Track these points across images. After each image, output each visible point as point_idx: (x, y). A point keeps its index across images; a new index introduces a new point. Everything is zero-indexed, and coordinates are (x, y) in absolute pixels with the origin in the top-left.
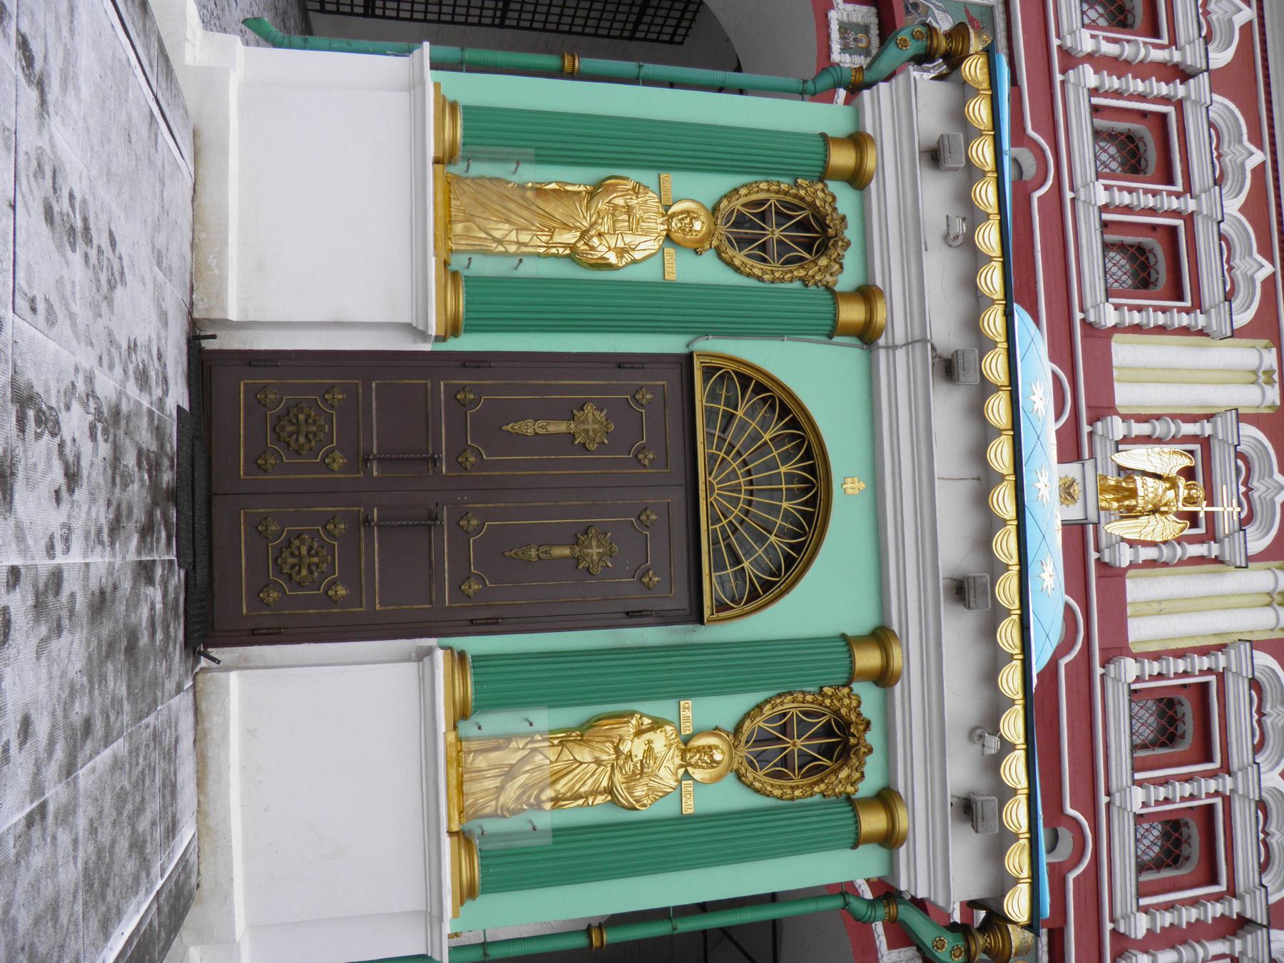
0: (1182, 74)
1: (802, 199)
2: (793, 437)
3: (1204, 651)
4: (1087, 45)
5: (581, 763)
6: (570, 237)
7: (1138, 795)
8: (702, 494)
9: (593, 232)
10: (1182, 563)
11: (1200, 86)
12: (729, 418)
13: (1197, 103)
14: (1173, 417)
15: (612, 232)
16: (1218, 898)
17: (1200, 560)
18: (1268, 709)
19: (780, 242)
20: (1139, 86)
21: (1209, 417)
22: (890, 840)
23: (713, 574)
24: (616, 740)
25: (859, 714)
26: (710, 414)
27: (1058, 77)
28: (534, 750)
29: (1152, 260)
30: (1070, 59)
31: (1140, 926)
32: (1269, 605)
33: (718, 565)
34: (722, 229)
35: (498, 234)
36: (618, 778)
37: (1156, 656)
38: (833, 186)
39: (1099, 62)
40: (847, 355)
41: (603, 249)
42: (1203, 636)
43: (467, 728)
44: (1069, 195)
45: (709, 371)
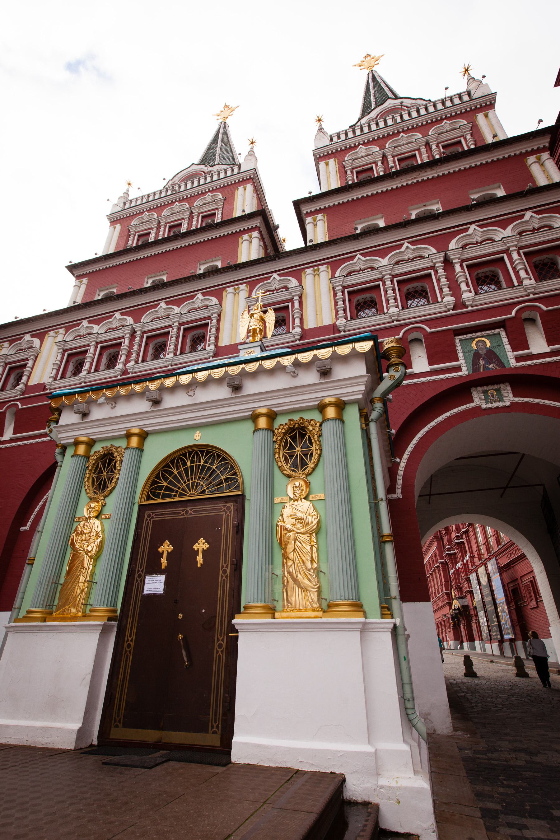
1: (94, 464)
2: (178, 461)
3: (335, 295)
5: (295, 549)
7: (393, 310)
9: (86, 549)
11: (138, 327)
12: (167, 489)
13: (143, 327)
15: (88, 541)
16: (436, 272)
17: (301, 303)
19: (107, 473)
20: (136, 347)
22: (341, 406)
23: (225, 491)
24: (286, 532)
25: (286, 424)
26: (165, 496)
27: (131, 375)
28: (289, 572)
29: (197, 336)
31: (450, 299)
32: (319, 275)
35: (79, 591)
36: (302, 530)
37: (337, 312)
38: (92, 453)
40: (150, 443)
42: (330, 297)
45: (148, 498)
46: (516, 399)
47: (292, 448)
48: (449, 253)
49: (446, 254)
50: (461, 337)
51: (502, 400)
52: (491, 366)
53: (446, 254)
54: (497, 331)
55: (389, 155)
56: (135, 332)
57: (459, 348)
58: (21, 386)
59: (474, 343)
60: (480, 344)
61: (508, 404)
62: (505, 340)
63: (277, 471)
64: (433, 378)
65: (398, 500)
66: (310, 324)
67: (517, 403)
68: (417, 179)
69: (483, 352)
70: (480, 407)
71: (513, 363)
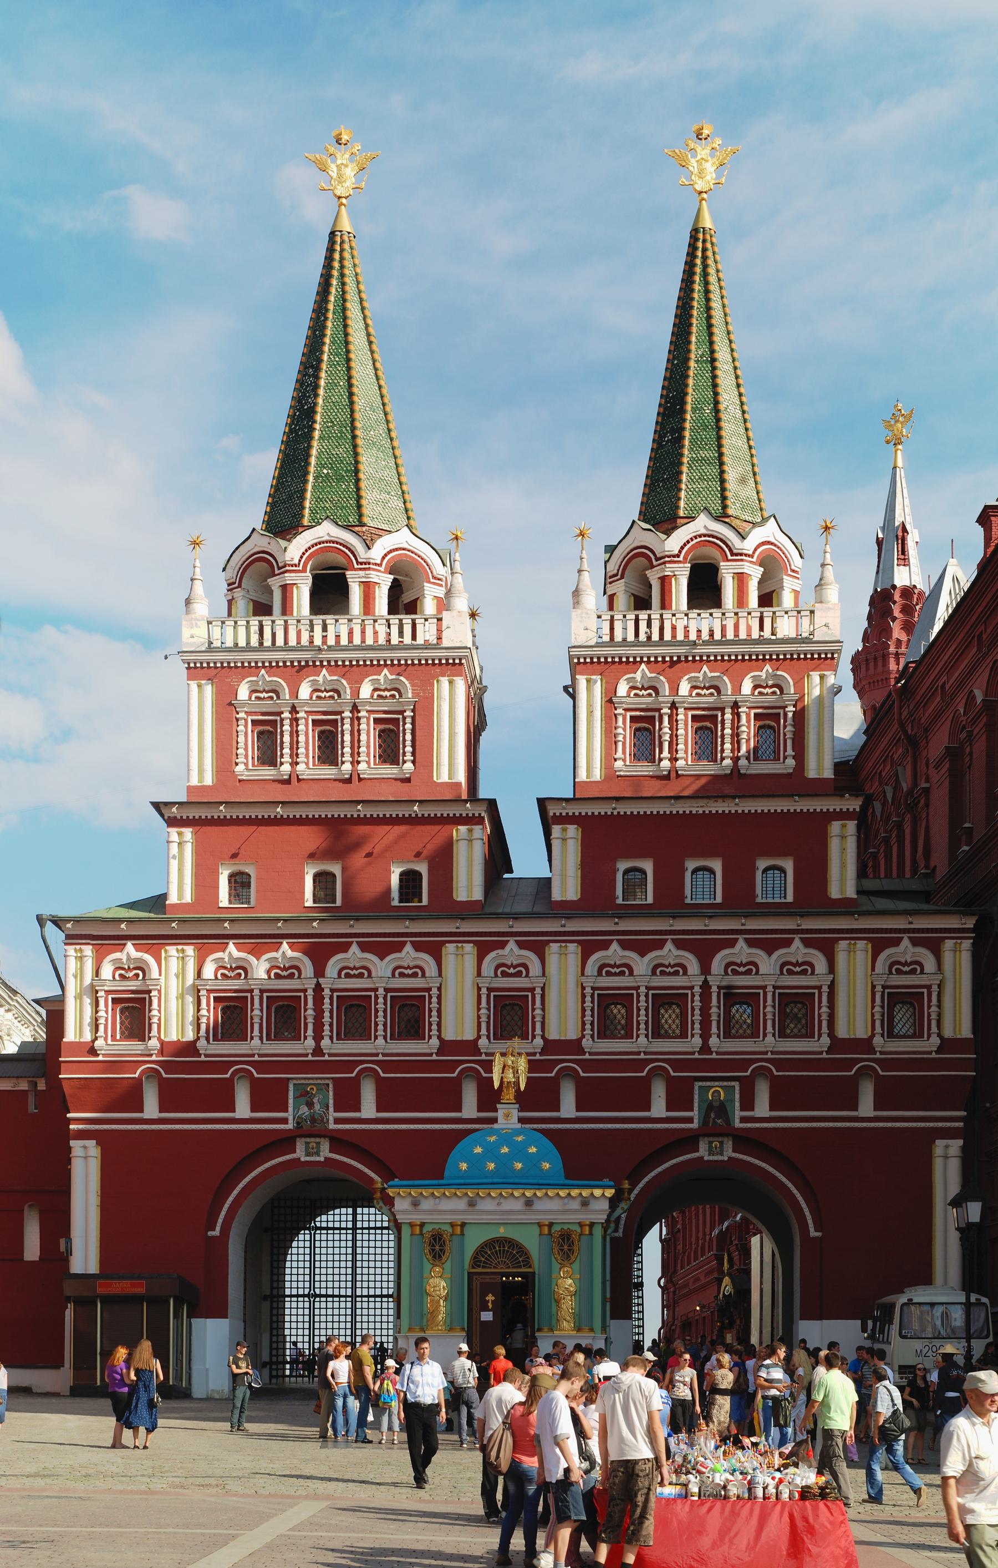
0: (318, 989)
3: (583, 996)
4: (310, 1043)
6: (442, 1301)
8: (503, 1270)
10: (543, 1009)
14: (479, 1009)
18: (612, 963)
21: (479, 989)
26: (484, 1267)
30: (318, 1051)
33: (520, 1267)
34: (437, 1262)
37: (584, 1024)
39: (318, 1037)
41: (444, 1293)
43: (554, 1329)
44: (380, 1058)
45: (473, 1268)
46: (734, 1155)
47: (562, 1246)
48: (709, 978)
49: (706, 979)
50: (701, 1084)
51: (722, 1154)
52: (719, 1121)
53: (706, 979)
54: (733, 1083)
55: (681, 707)
56: (323, 990)
57: (696, 1097)
58: (154, 1043)
59: (712, 1090)
60: (716, 1094)
61: (726, 1159)
62: (737, 1096)
63: (553, 1259)
64: (666, 1126)
65: (620, 1238)
66: (553, 1035)
67: (734, 1158)
68: (703, 809)
69: (716, 1104)
70: (703, 1157)
71: (737, 1124)
